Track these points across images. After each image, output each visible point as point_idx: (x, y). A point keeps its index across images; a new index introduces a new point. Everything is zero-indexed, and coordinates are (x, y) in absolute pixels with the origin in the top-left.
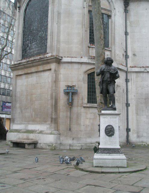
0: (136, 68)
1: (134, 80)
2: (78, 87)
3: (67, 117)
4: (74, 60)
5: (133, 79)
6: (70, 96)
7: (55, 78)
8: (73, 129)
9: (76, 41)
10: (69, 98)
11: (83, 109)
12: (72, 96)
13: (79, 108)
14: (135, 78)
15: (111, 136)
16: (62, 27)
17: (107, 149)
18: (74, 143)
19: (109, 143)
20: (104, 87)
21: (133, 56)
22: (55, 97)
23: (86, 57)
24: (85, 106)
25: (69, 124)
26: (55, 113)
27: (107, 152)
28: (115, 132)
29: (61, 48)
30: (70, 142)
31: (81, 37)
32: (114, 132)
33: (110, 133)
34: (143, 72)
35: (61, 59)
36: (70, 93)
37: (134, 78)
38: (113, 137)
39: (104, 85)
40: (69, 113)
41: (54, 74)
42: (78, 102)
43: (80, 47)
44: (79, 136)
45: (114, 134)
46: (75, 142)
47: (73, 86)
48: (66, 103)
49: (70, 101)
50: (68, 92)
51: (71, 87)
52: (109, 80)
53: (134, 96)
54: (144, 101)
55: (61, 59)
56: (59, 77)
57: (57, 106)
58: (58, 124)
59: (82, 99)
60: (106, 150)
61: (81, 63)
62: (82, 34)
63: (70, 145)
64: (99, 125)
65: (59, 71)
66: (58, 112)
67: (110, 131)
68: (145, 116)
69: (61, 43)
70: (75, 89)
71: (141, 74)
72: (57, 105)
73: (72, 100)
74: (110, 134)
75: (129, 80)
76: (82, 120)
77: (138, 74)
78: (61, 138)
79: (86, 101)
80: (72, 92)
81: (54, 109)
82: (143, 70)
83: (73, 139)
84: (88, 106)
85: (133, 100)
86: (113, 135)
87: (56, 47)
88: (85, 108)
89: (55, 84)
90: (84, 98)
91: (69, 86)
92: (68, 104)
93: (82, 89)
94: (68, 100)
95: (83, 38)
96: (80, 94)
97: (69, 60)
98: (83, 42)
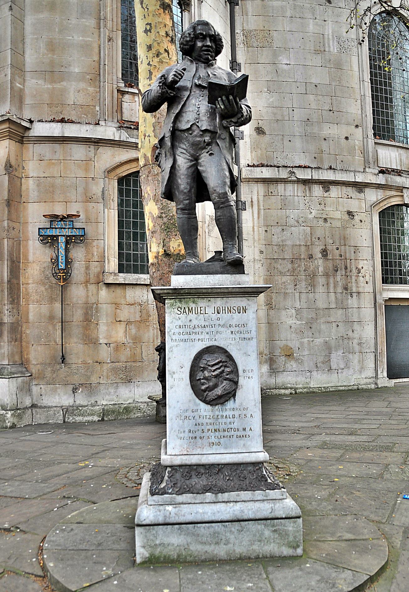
0: (264, 169)
1: (259, 206)
2: (88, 220)
3: (51, 318)
4: (71, 131)
5: (255, 203)
6: (62, 251)
7: (9, 191)
8: (72, 359)
9: (77, 70)
10: (57, 257)
11: (104, 293)
12: (67, 250)
13: (92, 288)
14: (261, 198)
15: (222, 404)
16: (29, 20)
17: (203, 465)
18: (78, 402)
19: (213, 440)
20: (183, 162)
21: (255, 133)
22: (11, 254)
23: (110, 124)
24: (110, 280)
25: (59, 341)
26: (10, 306)
27: (202, 482)
28: (241, 381)
29: (27, 91)
30: (66, 400)
31: (96, 58)
32: (236, 383)
33: (216, 386)
34: (284, 181)
35: (29, 129)
36: (62, 240)
37: (258, 198)
38: (230, 404)
39: (179, 151)
40: (58, 305)
41: (6, 177)
42: (87, 268)
43: (91, 89)
44: (94, 380)
45: (239, 394)
46: (81, 399)
47: (69, 216)
48: (49, 273)
49: (62, 266)
50: (52, 237)
51: (63, 219)
52: (205, 125)
53: (261, 252)
54: (290, 266)
55: (29, 129)
56: (24, 188)
57: (18, 284)
58: (24, 344)
59: (102, 260)
60: (199, 474)
61: (98, 142)
62: (97, 50)
63: (67, 411)
64: (161, 349)
65: (23, 168)
66: (22, 302)
67: (216, 376)
68: (293, 311)
69: (28, 76)
70: (77, 225)
71: (281, 187)
72: (18, 278)
73: (68, 262)
74: (219, 391)
75: (245, 203)
76: (103, 328)
77: (272, 187)
78: (35, 390)
79: (113, 264)
80: (68, 236)
81: (6, 293)
82: (284, 174)
83: (74, 390)
84: (121, 281)
85: (258, 265)
86: (234, 396)
87: (12, 88)
88: (112, 288)
89: (9, 211)
90: (106, 255)
91: (56, 216)
92: (55, 275)
93: (101, 226)
94: (55, 261)
95: (102, 63)
96: (95, 243)
97: (56, 130)
98: (101, 74)
